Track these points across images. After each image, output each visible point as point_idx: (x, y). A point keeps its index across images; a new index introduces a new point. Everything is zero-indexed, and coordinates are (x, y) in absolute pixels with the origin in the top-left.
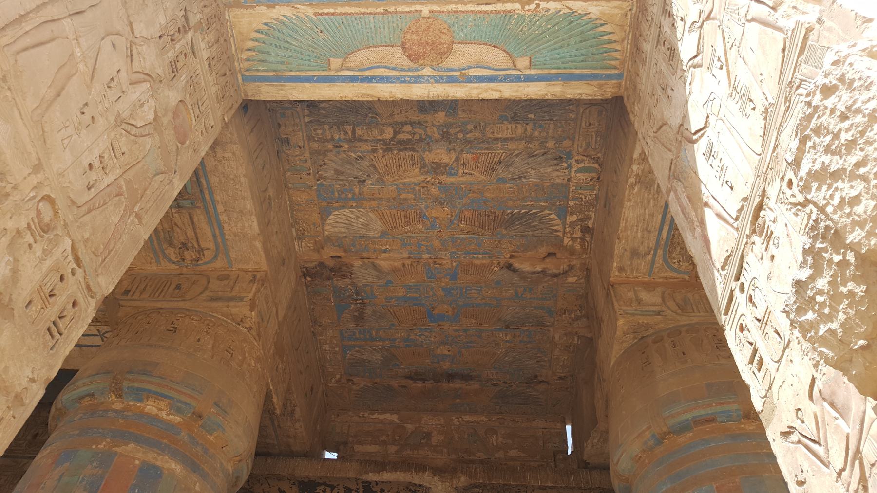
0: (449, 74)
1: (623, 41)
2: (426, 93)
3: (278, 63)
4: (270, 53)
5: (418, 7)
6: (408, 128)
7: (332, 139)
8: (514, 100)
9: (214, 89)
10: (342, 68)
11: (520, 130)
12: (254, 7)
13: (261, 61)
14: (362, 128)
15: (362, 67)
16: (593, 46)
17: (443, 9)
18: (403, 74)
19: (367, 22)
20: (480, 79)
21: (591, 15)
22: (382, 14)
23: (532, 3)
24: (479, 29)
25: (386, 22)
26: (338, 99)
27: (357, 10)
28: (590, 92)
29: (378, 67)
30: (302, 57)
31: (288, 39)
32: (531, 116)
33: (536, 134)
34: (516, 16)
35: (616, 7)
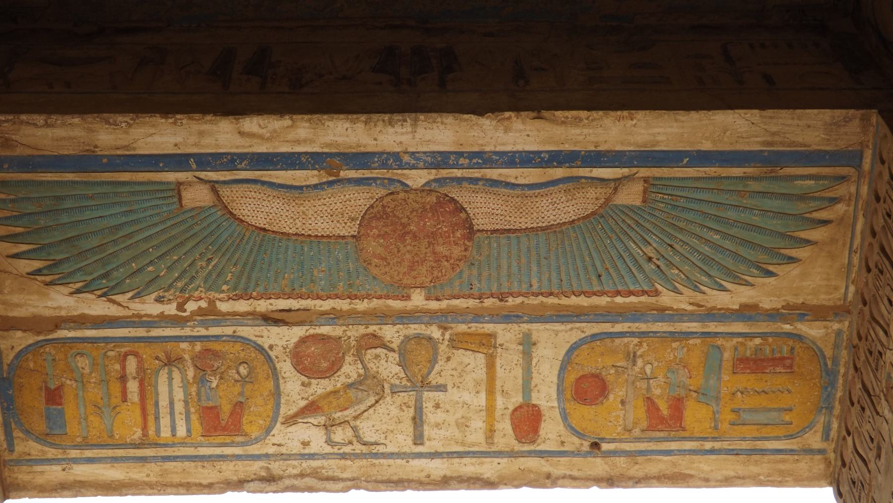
0: (367, 174)
3: (764, 194)
5: (434, 305)
10: (618, 181)
13: (803, 197)
15: (570, 185)
16: (46, 228)
17: (381, 302)
18: (476, 173)
19: (545, 277)
20: (291, 161)
21: (66, 290)
22: (511, 294)
23: (193, 313)
24: (302, 264)
26: (640, 114)
27: (565, 301)
28: (27, 130)
29: (531, 186)
30: (706, 209)
31: (727, 244)
34: (225, 287)
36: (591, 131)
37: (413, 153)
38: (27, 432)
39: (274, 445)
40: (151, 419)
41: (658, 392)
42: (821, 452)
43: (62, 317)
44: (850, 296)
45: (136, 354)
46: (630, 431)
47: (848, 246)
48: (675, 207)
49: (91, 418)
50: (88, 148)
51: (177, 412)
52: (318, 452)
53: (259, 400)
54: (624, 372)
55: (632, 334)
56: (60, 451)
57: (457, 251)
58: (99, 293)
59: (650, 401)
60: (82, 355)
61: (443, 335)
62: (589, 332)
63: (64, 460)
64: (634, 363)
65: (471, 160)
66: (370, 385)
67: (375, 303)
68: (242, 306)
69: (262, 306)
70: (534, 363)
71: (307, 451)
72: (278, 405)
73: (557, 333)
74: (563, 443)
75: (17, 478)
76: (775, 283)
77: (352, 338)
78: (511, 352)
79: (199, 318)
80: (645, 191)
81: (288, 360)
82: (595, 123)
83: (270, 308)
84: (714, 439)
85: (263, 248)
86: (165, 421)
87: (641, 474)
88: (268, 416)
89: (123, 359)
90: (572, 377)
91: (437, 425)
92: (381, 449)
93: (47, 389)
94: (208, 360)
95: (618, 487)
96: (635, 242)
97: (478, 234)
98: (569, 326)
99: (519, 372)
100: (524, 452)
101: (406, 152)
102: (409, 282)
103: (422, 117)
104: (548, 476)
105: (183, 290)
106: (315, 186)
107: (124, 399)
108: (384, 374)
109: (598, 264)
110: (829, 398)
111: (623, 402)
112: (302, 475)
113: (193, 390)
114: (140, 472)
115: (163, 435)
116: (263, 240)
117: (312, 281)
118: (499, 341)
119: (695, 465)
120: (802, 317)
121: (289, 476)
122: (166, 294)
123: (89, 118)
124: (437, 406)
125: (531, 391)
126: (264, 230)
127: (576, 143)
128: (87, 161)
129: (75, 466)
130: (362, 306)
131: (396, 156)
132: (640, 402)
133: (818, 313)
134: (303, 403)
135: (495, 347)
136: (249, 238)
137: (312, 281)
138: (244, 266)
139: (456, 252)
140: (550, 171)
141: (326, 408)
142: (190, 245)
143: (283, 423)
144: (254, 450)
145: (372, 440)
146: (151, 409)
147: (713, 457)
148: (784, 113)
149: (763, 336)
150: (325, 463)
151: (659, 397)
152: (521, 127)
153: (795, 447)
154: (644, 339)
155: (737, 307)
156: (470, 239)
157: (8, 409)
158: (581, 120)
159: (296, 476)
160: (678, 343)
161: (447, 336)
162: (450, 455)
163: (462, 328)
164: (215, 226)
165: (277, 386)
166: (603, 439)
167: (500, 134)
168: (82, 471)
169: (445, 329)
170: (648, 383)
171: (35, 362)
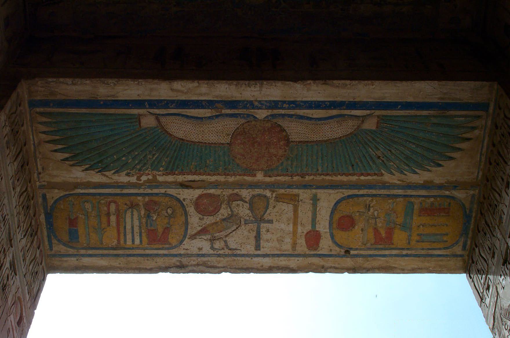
0: (236, 111)
1: (39, 144)
2: (264, 89)
5: (268, 179)
10: (364, 117)
12: (446, 183)
17: (241, 177)
18: (292, 112)
21: (80, 169)
22: (308, 174)
26: (377, 83)
29: (320, 119)
34: (161, 169)
36: (351, 91)
37: (260, 101)
38: (59, 240)
39: (184, 249)
40: (122, 235)
41: (380, 225)
42: (461, 256)
43: (77, 183)
44: (480, 177)
45: (115, 202)
46: (365, 245)
47: (480, 151)
49: (91, 234)
50: (93, 96)
55: (368, 195)
56: (76, 250)
57: (281, 152)
59: (376, 230)
61: (272, 194)
62: (346, 194)
63: (77, 255)
64: (369, 210)
65: (289, 105)
68: (170, 178)
69: (180, 178)
70: (317, 210)
71: (201, 253)
72: (187, 229)
73: (330, 194)
79: (148, 184)
80: (378, 123)
83: (184, 179)
84: (408, 249)
86: (129, 236)
87: (370, 266)
88: (182, 235)
89: (108, 205)
90: (336, 217)
91: (267, 241)
92: (238, 252)
93: (70, 219)
94: (151, 207)
95: (358, 273)
96: (372, 149)
98: (337, 191)
99: (310, 214)
101: (256, 101)
102: (256, 167)
103: (265, 83)
104: (323, 267)
105: (140, 170)
106: (209, 118)
107: (109, 225)
108: (241, 214)
109: (352, 159)
111: (362, 230)
112: (198, 265)
113: (144, 220)
115: (128, 243)
117: (206, 166)
118: (301, 198)
120: (455, 187)
121: (191, 265)
122: (131, 172)
124: (268, 231)
126: (182, 139)
128: (93, 103)
129: (83, 258)
130: (231, 179)
131: (251, 103)
132: (371, 230)
135: (298, 201)
138: (172, 158)
141: (211, 230)
143: (189, 238)
144: (174, 251)
145: (234, 248)
147: (406, 258)
148: (451, 83)
150: (209, 259)
151: (380, 227)
153: (448, 253)
154: (374, 198)
155: (422, 182)
156: (287, 146)
159: (195, 265)
161: (274, 195)
162: (274, 255)
163: (282, 191)
166: (351, 249)
169: (273, 192)
170: (376, 221)
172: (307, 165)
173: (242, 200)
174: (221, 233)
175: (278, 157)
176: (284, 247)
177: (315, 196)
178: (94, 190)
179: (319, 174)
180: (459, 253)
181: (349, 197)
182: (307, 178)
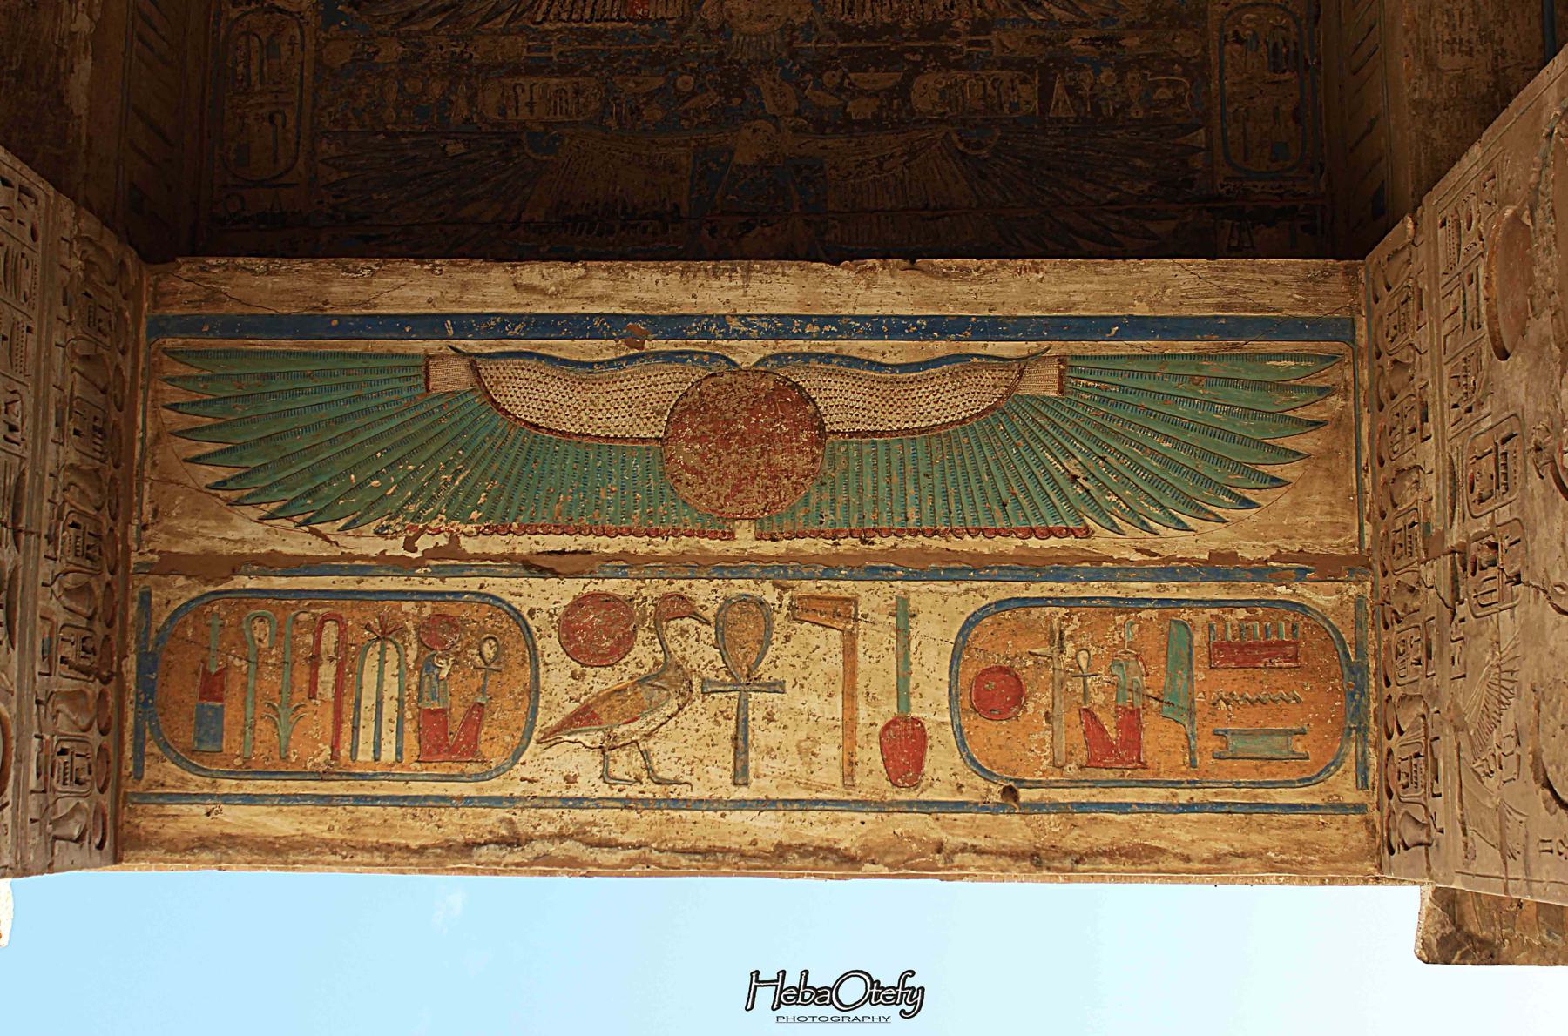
1: (157, 439)
2: (754, 284)
4: (1247, 412)
5: (768, 548)
6: (860, 109)
7: (1121, 69)
8: (473, 258)
9: (1423, 338)
10: (1022, 364)
11: (490, 98)
12: (1273, 558)
13: (1281, 387)
14: (1014, 107)
17: (692, 541)
18: (828, 347)
19: (926, 506)
20: (580, 326)
21: (255, 513)
22: (879, 532)
25: (868, 507)
26: (1048, 264)
27: (955, 544)
29: (904, 368)
31: (1183, 457)
32: (455, 148)
33: (436, 89)
34: (475, 515)
35: (188, 536)
37: (744, 316)
38: (165, 746)
39: (523, 779)
40: (347, 727)
41: (1099, 699)
42: (1359, 808)
45: (339, 620)
46: (1062, 767)
48: (1104, 400)
49: (261, 725)
51: (385, 719)
52: (587, 794)
53: (507, 702)
54: (1047, 666)
55: (1057, 602)
56: (209, 780)
57: (802, 463)
58: (299, 519)
60: (262, 618)
61: (780, 598)
63: (211, 796)
64: (1062, 650)
66: (671, 677)
67: (684, 544)
68: (496, 545)
69: (525, 545)
70: (913, 649)
71: (571, 793)
73: (946, 597)
74: (960, 786)
75: (137, 826)
76: (1256, 518)
77: (650, 601)
78: (879, 627)
79: (434, 563)
80: (1061, 374)
81: (555, 635)
82: (987, 276)
84: (1192, 784)
85: (533, 454)
86: (366, 734)
87: (1082, 846)
89: (318, 628)
90: (971, 672)
92: (684, 792)
94: (439, 631)
96: (1051, 453)
97: (831, 438)
99: (891, 661)
100: (902, 802)
103: (757, 266)
105: (416, 517)
106: (610, 363)
107: (312, 695)
110: (1359, 712)
112: (561, 837)
114: (319, 822)
115: (360, 758)
116: (534, 442)
117: (597, 507)
119: (1166, 831)
120: (1301, 575)
121: (542, 837)
123: (323, 263)
125: (909, 695)
126: (537, 427)
127: (964, 304)
128: (309, 325)
130: (665, 547)
133: (1326, 568)
134: (571, 707)
135: (856, 620)
136: (515, 439)
137: (597, 507)
138: (504, 482)
139: (799, 464)
140: (931, 345)
141: (604, 716)
142: (433, 448)
143: (539, 742)
144: (492, 788)
145: (671, 776)
146: (348, 714)
149: (1249, 605)
150: (598, 814)
152: (890, 281)
153: (1317, 801)
156: (820, 445)
157: (145, 704)
158: (969, 272)
159: (551, 838)
160: (1124, 617)
161: (786, 601)
162: (788, 804)
163: (808, 587)
164: (470, 419)
165: (536, 677)
166: (1020, 781)
167: (861, 290)
168: (236, 818)
169: (784, 589)
170: (1085, 683)
171: (195, 629)
172: (875, 502)
173: (697, 617)
174: (634, 726)
175: (794, 478)
176: (820, 777)
177: (903, 601)
178: (284, 580)
179: (910, 532)
180: (1351, 797)
181: (999, 603)
182: (880, 543)
